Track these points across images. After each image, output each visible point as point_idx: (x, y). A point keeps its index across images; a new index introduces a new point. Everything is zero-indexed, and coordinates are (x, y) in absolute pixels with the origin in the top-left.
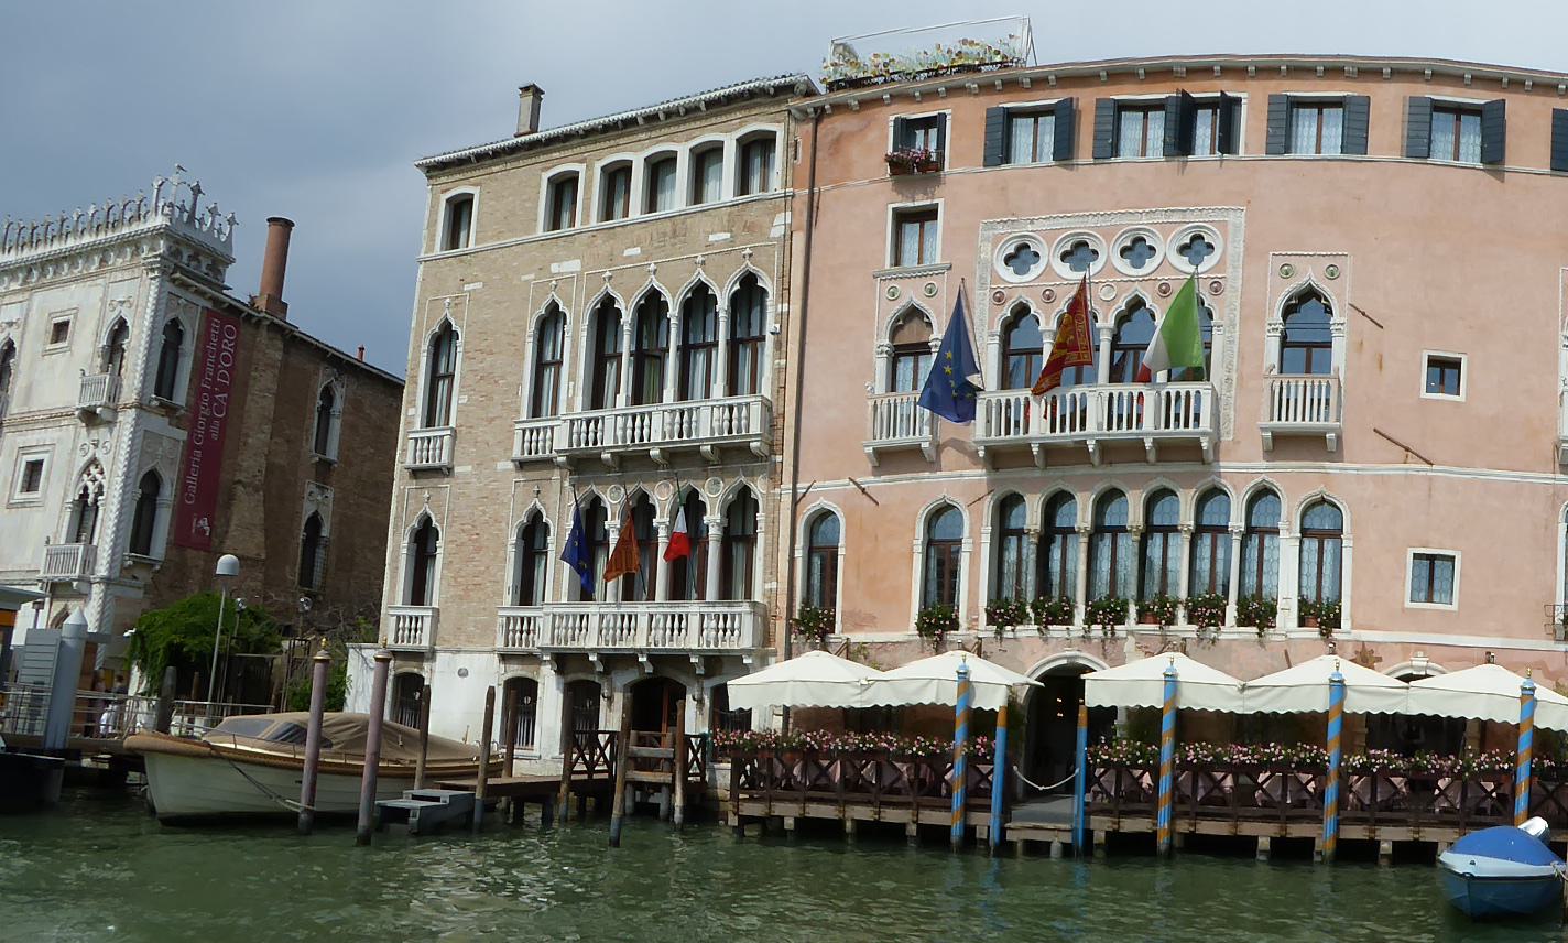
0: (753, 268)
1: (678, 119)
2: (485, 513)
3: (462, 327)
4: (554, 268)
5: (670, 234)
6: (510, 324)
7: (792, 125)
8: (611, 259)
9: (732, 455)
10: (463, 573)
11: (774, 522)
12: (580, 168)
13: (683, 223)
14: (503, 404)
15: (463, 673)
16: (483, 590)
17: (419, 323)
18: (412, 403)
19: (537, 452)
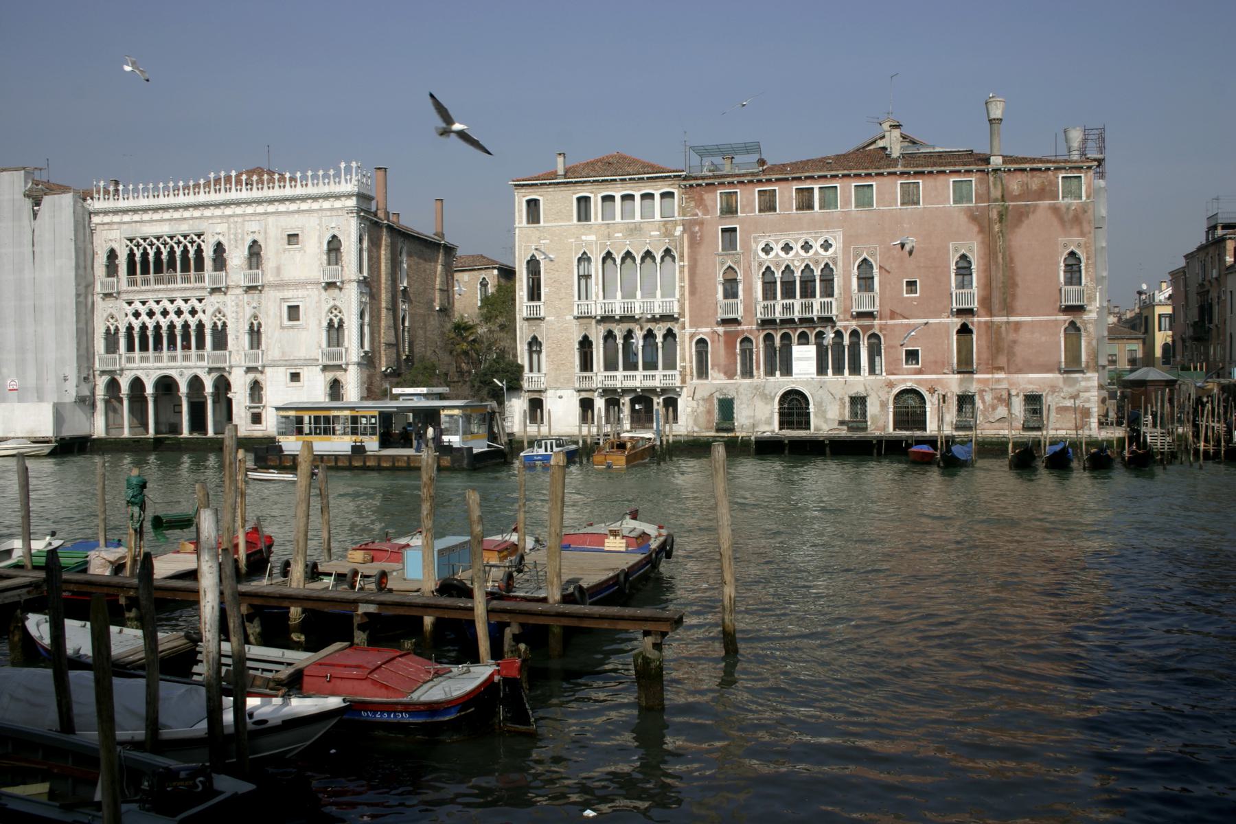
4: (584, 238)
12: (591, 195)
15: (561, 397)
17: (520, 255)
18: (521, 290)
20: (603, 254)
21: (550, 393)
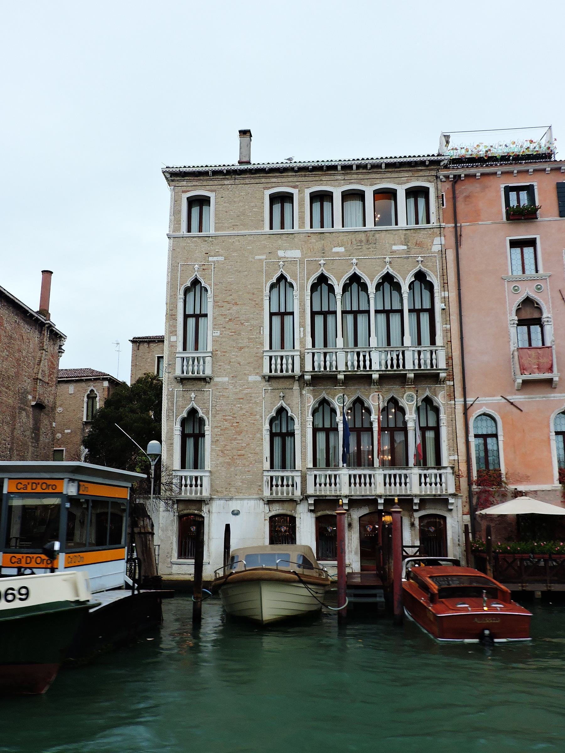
0: (424, 269)
1: (365, 171)
2: (241, 409)
3: (210, 285)
4: (281, 253)
5: (364, 241)
6: (249, 287)
7: (439, 183)
8: (323, 252)
9: (429, 377)
10: (228, 448)
11: (452, 421)
12: (295, 192)
13: (373, 236)
14: (249, 339)
16: (245, 459)
19: (287, 371)
20: (313, 279)
21: (216, 506)
